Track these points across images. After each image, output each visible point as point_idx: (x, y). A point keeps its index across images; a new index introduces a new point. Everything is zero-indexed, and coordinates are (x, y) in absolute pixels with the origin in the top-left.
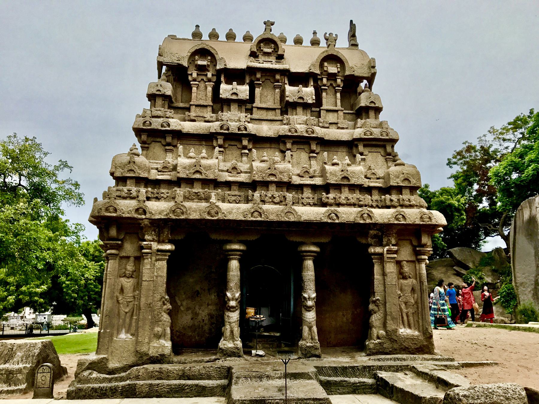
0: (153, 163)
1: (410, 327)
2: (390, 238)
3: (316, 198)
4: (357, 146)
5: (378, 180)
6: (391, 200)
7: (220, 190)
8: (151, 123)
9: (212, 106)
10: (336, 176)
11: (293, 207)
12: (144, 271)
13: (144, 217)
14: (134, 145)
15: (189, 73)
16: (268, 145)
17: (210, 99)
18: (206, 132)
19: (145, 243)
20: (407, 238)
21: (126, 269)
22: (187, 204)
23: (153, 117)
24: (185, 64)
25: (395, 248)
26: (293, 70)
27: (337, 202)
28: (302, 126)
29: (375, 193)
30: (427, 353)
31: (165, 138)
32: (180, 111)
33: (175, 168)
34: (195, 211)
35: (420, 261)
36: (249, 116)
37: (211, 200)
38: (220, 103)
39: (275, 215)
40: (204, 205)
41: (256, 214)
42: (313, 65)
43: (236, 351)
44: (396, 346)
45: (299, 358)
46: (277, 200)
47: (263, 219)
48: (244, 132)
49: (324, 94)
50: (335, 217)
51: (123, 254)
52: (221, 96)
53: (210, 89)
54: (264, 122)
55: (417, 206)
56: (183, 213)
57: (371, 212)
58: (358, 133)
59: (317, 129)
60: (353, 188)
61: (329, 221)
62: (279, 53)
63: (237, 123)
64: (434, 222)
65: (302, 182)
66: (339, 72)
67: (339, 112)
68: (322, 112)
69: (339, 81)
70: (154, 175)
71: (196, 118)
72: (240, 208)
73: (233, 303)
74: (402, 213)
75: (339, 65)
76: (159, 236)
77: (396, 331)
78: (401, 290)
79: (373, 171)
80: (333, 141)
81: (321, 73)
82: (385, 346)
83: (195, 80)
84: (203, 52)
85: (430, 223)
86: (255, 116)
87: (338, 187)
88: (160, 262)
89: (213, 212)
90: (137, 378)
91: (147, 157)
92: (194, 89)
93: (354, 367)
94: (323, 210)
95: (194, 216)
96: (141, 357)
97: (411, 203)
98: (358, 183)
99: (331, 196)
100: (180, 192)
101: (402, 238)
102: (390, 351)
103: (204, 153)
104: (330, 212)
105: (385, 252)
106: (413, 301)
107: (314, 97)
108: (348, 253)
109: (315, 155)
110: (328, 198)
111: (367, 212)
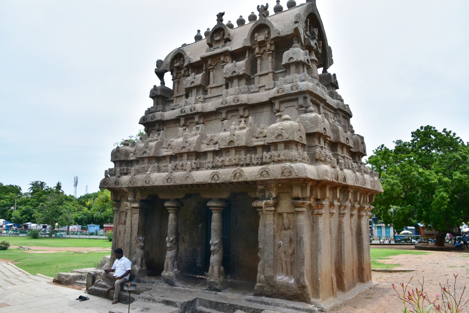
2: (271, 192)
10: (225, 141)
16: (214, 118)
29: (260, 150)
34: (139, 181)
36: (202, 96)
39: (179, 180)
44: (275, 291)
45: (206, 290)
48: (194, 112)
49: (259, 61)
50: (217, 178)
51: (121, 210)
55: (286, 160)
61: (213, 182)
62: (226, 37)
64: (293, 176)
69: (268, 46)
71: (175, 107)
74: (266, 170)
76: (135, 197)
77: (272, 278)
79: (261, 130)
82: (265, 289)
85: (291, 177)
87: (226, 150)
89: (147, 181)
93: (224, 303)
94: (209, 172)
95: (139, 184)
97: (279, 159)
104: (214, 174)
105: (263, 206)
106: (291, 251)
111: (239, 171)
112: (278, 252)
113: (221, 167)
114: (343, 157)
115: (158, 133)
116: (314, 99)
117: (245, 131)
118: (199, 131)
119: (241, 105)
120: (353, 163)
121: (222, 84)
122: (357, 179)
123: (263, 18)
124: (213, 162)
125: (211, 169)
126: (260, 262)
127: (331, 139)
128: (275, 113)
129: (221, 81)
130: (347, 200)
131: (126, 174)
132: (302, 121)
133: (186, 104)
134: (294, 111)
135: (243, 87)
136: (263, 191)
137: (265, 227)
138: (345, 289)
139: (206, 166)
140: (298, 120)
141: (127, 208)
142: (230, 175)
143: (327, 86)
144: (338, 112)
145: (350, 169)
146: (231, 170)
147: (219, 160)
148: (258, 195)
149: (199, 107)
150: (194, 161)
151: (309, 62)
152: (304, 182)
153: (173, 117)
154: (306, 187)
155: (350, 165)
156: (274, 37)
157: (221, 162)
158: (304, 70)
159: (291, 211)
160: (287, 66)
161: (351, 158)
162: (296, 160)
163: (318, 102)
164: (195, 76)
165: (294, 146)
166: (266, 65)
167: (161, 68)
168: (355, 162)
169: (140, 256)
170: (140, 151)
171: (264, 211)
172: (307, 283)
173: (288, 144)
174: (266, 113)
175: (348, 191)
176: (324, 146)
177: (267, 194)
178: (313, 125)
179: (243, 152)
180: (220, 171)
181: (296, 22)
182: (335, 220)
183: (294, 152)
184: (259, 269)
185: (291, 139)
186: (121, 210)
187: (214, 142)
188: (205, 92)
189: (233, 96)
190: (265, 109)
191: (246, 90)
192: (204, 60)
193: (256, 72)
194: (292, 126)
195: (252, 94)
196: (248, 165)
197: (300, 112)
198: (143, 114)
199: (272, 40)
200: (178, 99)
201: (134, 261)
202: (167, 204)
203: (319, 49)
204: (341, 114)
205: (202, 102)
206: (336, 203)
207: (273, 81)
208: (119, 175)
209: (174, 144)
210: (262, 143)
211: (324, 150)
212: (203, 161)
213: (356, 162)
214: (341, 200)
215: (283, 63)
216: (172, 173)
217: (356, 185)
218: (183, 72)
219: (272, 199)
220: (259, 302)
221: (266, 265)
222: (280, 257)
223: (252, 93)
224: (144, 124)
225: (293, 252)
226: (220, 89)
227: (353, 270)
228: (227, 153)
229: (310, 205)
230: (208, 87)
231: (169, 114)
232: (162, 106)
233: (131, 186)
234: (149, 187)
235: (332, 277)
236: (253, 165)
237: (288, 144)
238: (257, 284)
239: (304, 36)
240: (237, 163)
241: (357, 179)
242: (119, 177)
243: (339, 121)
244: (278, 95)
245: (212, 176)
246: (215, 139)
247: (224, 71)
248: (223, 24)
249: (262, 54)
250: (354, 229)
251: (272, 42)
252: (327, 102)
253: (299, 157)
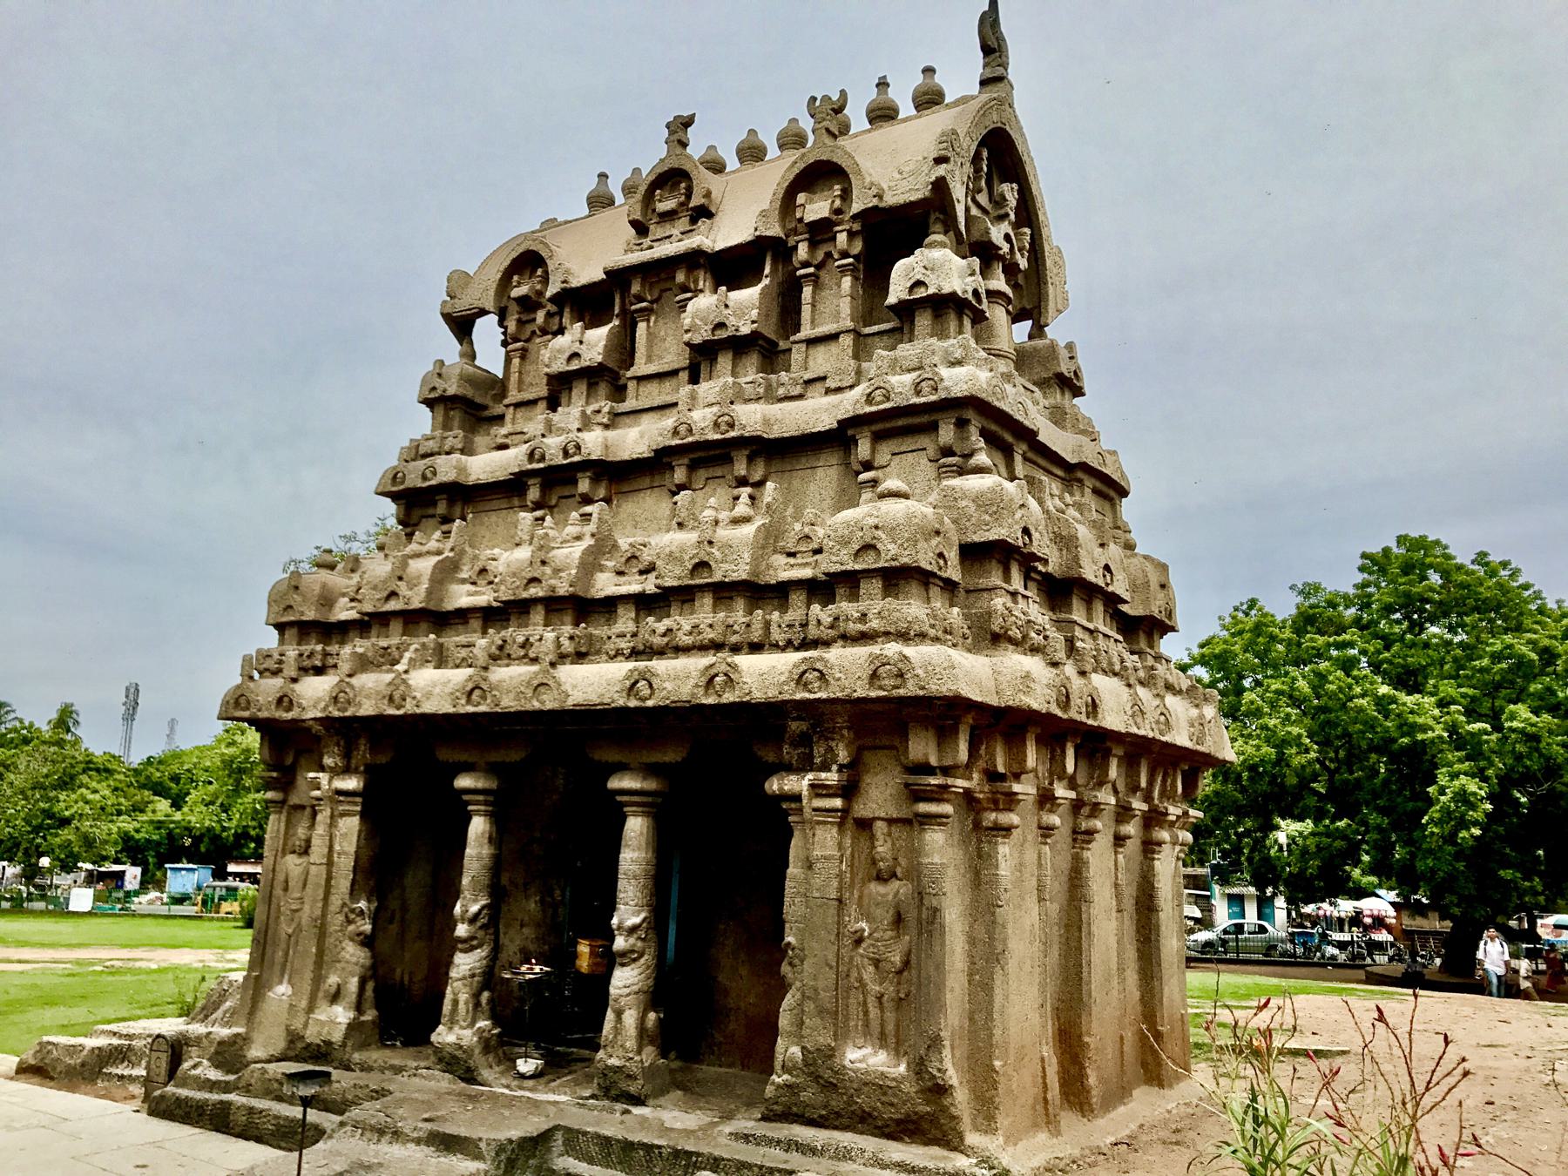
2: (833, 744)
16: (647, 481)
27: (674, 643)
29: (797, 598)
34: (368, 697)
36: (606, 406)
39: (512, 696)
42: (763, 214)
44: (837, 1103)
45: (593, 1097)
48: (576, 459)
49: (807, 292)
50: (647, 692)
51: (294, 800)
55: (887, 634)
57: (734, 667)
60: (724, 592)
61: (633, 703)
64: (910, 689)
69: (842, 238)
71: (508, 441)
74: (819, 665)
76: (347, 755)
77: (830, 1054)
79: (806, 530)
80: (792, 438)
82: (805, 1096)
85: (902, 692)
86: (630, 404)
87: (682, 596)
89: (397, 696)
93: (653, 1146)
94: (621, 669)
95: (367, 709)
98: (735, 577)
101: (868, 741)
102: (821, 1116)
105: (805, 793)
106: (897, 959)
111: (724, 668)
112: (852, 958)
113: (660, 653)
114: (1091, 632)
115: (445, 528)
116: (994, 427)
117: (748, 530)
118: (592, 527)
119: (741, 442)
120: (1126, 655)
121: (676, 366)
122: (1138, 711)
123: (828, 141)
124: (634, 635)
125: (628, 658)
126: (789, 996)
127: (1050, 569)
128: (858, 473)
129: (673, 355)
130: (1100, 784)
131: (319, 671)
132: (949, 501)
133: (550, 428)
134: (923, 466)
135: (749, 379)
136: (804, 740)
137: (810, 867)
138: (1090, 1105)
139: (610, 647)
140: (934, 497)
141: (317, 793)
142: (692, 682)
143: (1042, 384)
144: (1080, 475)
145: (1115, 674)
146: (696, 664)
147: (657, 626)
149: (594, 443)
150: (568, 629)
151: (979, 301)
152: (945, 714)
153: (501, 476)
154: (955, 731)
155: (1116, 660)
156: (863, 207)
157: (664, 635)
158: (961, 325)
160: (906, 311)
161: (1120, 638)
162: (922, 636)
163: (1009, 438)
164: (583, 334)
165: (914, 588)
166: (833, 305)
167: (463, 304)
168: (1132, 653)
169: (358, 970)
170: (375, 588)
171: (807, 811)
172: (953, 1077)
173: (896, 578)
174: (824, 476)
175: (1107, 755)
176: (1022, 590)
177: (819, 752)
178: (987, 518)
179: (740, 604)
180: (659, 665)
181: (940, 160)
182: (1054, 857)
183: (913, 608)
184: (784, 1021)
185: (905, 560)
186: (294, 800)
187: (641, 567)
188: (619, 392)
189: (715, 409)
190: (823, 456)
191: (761, 390)
192: (618, 278)
193: (797, 328)
194: (910, 517)
195: (780, 405)
196: (756, 648)
197: (943, 472)
198: (393, 461)
199: (855, 217)
200: (520, 413)
201: (333, 990)
202: (464, 782)
203: (1018, 256)
204: (1090, 482)
205: (607, 427)
206: (1061, 791)
207: (852, 362)
208: (293, 674)
209: (501, 569)
210: (807, 573)
211: (1022, 603)
212: (599, 631)
213: (1140, 653)
214: (1080, 780)
215: (892, 299)
216: (486, 669)
217: (1134, 730)
218: (540, 316)
219: (835, 767)
220: (779, 1142)
221: (810, 1006)
222: (860, 980)
223: (781, 400)
224: (394, 496)
225: (906, 963)
226: (668, 384)
227: (1122, 1038)
228: (686, 606)
229: (968, 793)
230: (629, 374)
231: (486, 465)
232: (461, 433)
233: (336, 714)
234: (405, 716)
235: (1043, 1060)
236: (776, 647)
237: (896, 578)
238: (774, 1077)
239: (967, 210)
240: (719, 639)
241: (1138, 711)
242: (295, 680)
243: (1079, 507)
244: (868, 409)
245: (628, 683)
246: (646, 557)
247: (687, 321)
248: (689, 157)
249: (819, 267)
250: (1130, 892)
251: (856, 227)
252: (1041, 438)
253: (932, 626)
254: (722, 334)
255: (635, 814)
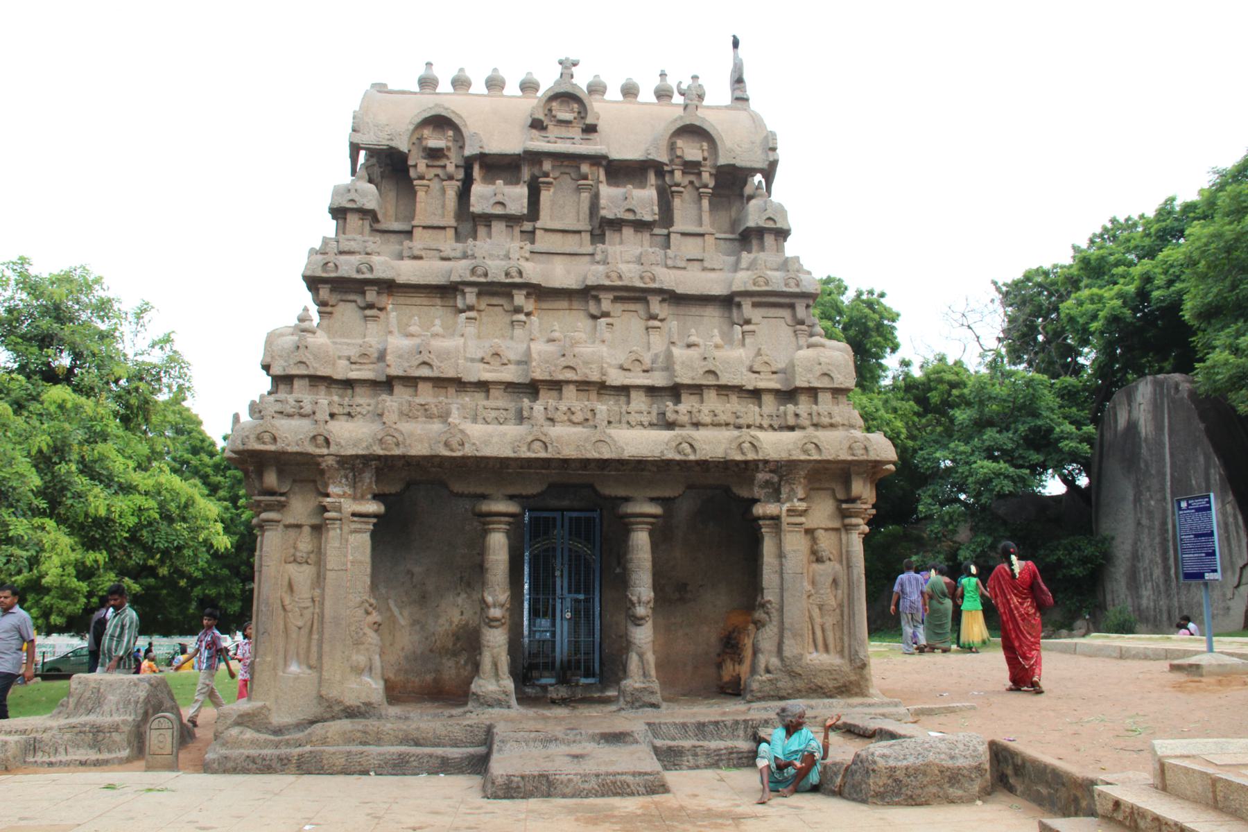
0: (345, 344)
1: (827, 649)
3: (654, 413)
4: (739, 305)
5: (775, 376)
6: (797, 415)
7: (467, 399)
8: (336, 266)
9: (456, 229)
11: (608, 431)
12: (329, 552)
13: (325, 451)
14: (306, 309)
15: (411, 162)
17: (452, 214)
18: (441, 281)
19: (328, 500)
20: (827, 485)
21: (295, 548)
22: (406, 427)
23: (341, 253)
24: (404, 147)
25: (802, 506)
26: (615, 155)
27: (694, 420)
28: (632, 266)
29: (768, 400)
30: (856, 695)
31: (363, 293)
32: (393, 237)
33: (382, 357)
35: (848, 528)
36: (528, 247)
37: (450, 420)
38: (470, 222)
40: (436, 427)
41: (537, 445)
43: (502, 697)
44: (799, 684)
46: (578, 417)
47: (549, 456)
48: (518, 280)
49: (677, 202)
50: (688, 450)
51: (291, 521)
52: (472, 209)
53: (451, 194)
54: (558, 260)
56: (397, 444)
58: (742, 280)
59: (660, 271)
61: (678, 457)
62: (589, 121)
63: (503, 263)
64: (873, 456)
65: (627, 382)
66: (705, 159)
67: (707, 237)
68: (672, 236)
69: (706, 177)
70: (342, 371)
71: (423, 253)
72: (505, 434)
73: (496, 612)
75: (705, 145)
76: (354, 485)
77: (800, 657)
78: (813, 583)
79: (766, 359)
81: (671, 161)
83: (422, 178)
84: (440, 122)
86: (538, 247)
87: (697, 389)
88: (358, 536)
89: (454, 442)
90: (324, 741)
91: (330, 331)
92: (421, 195)
94: (666, 435)
95: (419, 449)
96: (330, 707)
97: (833, 421)
99: (682, 408)
100: (393, 402)
101: (817, 485)
103: (437, 329)
104: (680, 440)
105: (784, 514)
106: (834, 603)
107: (656, 209)
108: (720, 514)
109: (656, 323)
110: (677, 412)
119: (660, 291)
148: (758, 492)
159: (831, 525)
177: (785, 491)
188: (531, 235)
202: (487, 507)
234: (463, 458)
240: (728, 420)
245: (674, 444)
254: (630, 216)
255: (642, 530)
